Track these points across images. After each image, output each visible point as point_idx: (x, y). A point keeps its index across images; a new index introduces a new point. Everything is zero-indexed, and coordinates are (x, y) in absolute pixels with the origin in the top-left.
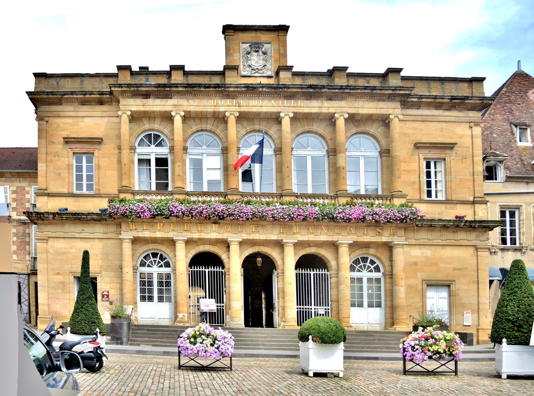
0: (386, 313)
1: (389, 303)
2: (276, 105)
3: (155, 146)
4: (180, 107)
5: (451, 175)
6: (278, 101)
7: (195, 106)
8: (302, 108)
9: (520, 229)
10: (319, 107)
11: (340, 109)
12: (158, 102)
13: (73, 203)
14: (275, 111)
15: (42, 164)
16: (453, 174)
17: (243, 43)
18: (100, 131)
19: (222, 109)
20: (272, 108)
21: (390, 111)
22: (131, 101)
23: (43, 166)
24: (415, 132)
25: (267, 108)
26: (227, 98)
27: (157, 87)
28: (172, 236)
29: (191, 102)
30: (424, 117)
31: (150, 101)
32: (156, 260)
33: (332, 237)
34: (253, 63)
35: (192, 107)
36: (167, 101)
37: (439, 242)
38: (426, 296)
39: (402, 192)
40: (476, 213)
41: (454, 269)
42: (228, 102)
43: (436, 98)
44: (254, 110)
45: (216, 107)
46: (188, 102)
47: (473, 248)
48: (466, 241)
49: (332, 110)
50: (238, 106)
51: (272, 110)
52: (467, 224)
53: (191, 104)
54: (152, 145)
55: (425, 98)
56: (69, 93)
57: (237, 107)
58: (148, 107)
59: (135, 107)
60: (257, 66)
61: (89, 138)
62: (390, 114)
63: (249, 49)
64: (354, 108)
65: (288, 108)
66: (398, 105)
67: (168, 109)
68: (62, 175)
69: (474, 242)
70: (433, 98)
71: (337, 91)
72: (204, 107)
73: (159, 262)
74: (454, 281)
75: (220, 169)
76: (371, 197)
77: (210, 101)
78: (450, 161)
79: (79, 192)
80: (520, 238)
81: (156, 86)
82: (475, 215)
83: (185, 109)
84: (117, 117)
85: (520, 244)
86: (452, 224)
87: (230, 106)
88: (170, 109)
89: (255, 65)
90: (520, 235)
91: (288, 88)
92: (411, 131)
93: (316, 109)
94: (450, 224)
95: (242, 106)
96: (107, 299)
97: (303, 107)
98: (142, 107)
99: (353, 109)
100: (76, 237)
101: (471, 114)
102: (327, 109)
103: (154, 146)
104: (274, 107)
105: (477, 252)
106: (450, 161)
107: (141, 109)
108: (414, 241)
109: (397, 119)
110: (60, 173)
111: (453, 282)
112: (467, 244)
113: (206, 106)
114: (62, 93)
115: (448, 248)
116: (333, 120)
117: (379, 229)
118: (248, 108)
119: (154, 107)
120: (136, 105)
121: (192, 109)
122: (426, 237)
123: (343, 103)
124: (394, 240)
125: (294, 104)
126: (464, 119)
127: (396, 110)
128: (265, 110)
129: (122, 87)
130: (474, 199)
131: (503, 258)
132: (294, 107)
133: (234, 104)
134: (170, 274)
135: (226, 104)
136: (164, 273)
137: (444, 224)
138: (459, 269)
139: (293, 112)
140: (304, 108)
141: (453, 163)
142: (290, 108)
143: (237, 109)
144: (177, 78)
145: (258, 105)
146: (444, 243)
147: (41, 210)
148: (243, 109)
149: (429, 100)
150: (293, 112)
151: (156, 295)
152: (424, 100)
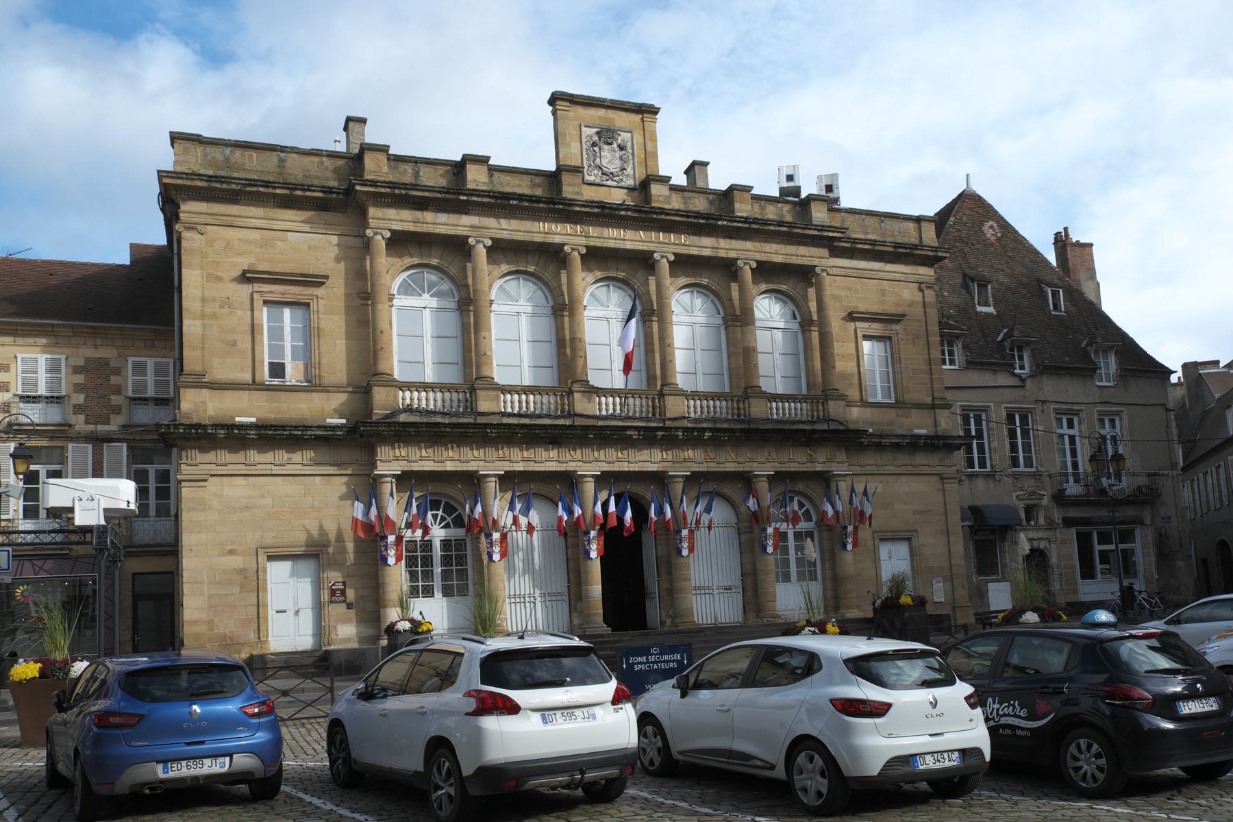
0: (824, 590)
1: (828, 572)
2: (647, 240)
3: (431, 296)
4: (484, 230)
5: (900, 363)
6: (649, 233)
7: (512, 230)
8: (688, 248)
9: (989, 442)
10: (713, 248)
11: (744, 252)
12: (443, 217)
13: (266, 404)
14: (645, 248)
15: (192, 322)
16: (903, 362)
17: (585, 126)
18: (322, 261)
19: (557, 239)
20: (641, 244)
21: (816, 262)
22: (392, 213)
23: (195, 325)
24: (848, 294)
25: (634, 243)
26: (566, 222)
27: (444, 193)
28: (475, 469)
29: (504, 223)
30: (860, 271)
31: (429, 216)
32: (437, 515)
33: (742, 465)
34: (604, 162)
35: (505, 232)
36: (460, 218)
37: (891, 469)
38: (879, 558)
39: (838, 390)
40: (938, 423)
41: (915, 513)
42: (569, 228)
43: (875, 245)
44: (612, 244)
45: (549, 236)
46: (499, 223)
47: (936, 478)
48: (927, 468)
49: (732, 255)
50: (585, 236)
51: (640, 248)
52: (929, 441)
53: (503, 227)
54: (428, 293)
55: (862, 243)
56: (259, 183)
57: (584, 238)
58: (425, 225)
59: (400, 223)
60: (610, 168)
61: (302, 275)
62: (815, 266)
63: (596, 138)
64: (764, 252)
65: (666, 246)
66: (825, 252)
67: (461, 231)
68: (240, 346)
69: (938, 468)
70: (871, 244)
71: (740, 225)
72: (526, 234)
73: (443, 519)
74: (916, 531)
75: (551, 342)
76: (796, 398)
77: (536, 224)
78: (898, 341)
79: (276, 382)
80: (991, 457)
81: (442, 190)
82: (936, 426)
83: (493, 235)
84: (356, 236)
85: (992, 466)
86: (908, 441)
87: (572, 235)
88: (465, 233)
89: (608, 166)
90: (990, 453)
91: (667, 214)
92: (843, 293)
93: (709, 250)
94: (906, 441)
95: (592, 237)
96: (342, 598)
97: (689, 246)
98: (412, 224)
99: (763, 254)
100: (274, 472)
101: (922, 270)
102: (724, 251)
103: (428, 295)
104: (643, 242)
105: (943, 484)
106: (898, 341)
107: (410, 227)
108: (858, 468)
109: (825, 274)
110: (235, 341)
111: (915, 533)
112: (929, 472)
113: (531, 232)
114: (244, 182)
115: (904, 478)
116: (733, 269)
117: (810, 450)
118: (602, 240)
119: (435, 226)
120: (401, 221)
121: (505, 235)
122: (873, 462)
123: (748, 245)
124: (832, 469)
125: (675, 240)
126: (913, 280)
127: (824, 260)
128: (629, 246)
129: (377, 186)
130: (933, 401)
131: (971, 489)
132: (674, 244)
133: (579, 233)
134: (465, 540)
135: (564, 232)
136: (453, 539)
137: (897, 441)
138: (921, 512)
139: (674, 254)
140: (691, 248)
141: (902, 346)
142: (670, 246)
143: (583, 241)
144: (476, 178)
145: (618, 237)
146: (898, 470)
147: (192, 418)
148: (593, 242)
149: (866, 247)
150: (674, 254)
151: (437, 583)
152: (859, 246)
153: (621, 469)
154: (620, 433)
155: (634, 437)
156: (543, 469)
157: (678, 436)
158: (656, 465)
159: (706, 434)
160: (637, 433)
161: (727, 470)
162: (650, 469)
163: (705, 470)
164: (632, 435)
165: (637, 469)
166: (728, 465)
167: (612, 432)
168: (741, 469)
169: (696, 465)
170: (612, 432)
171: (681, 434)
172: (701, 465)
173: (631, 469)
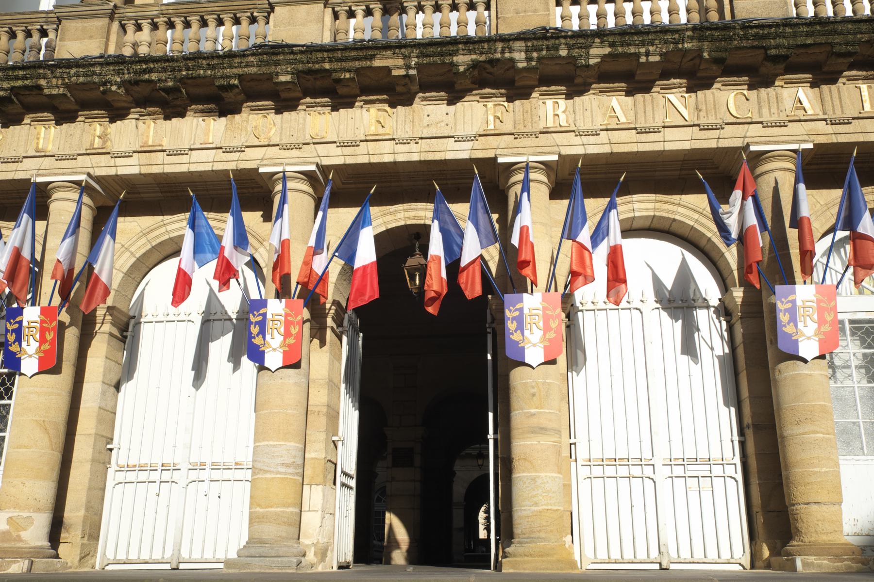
153: (375, 159)
154: (357, 64)
155: (395, 73)
156: (184, 169)
157: (512, 60)
158: (468, 145)
159: (593, 51)
160: (400, 62)
161: (669, 146)
162: (450, 156)
163: (606, 149)
164: (388, 70)
165: (415, 157)
166: (669, 134)
167: (337, 66)
168: (713, 144)
169: (578, 140)
170: (337, 66)
171: (523, 55)
172: (592, 139)
173: (401, 158)
